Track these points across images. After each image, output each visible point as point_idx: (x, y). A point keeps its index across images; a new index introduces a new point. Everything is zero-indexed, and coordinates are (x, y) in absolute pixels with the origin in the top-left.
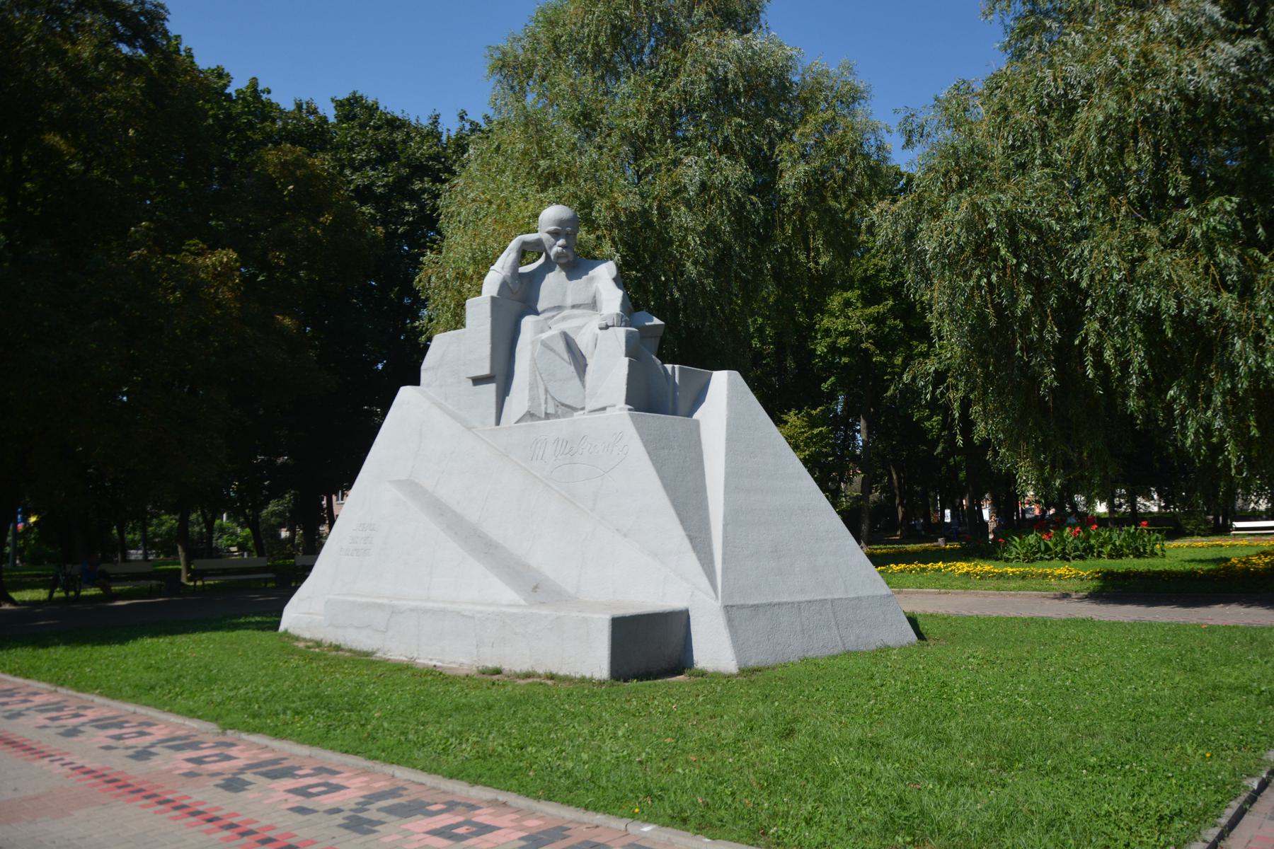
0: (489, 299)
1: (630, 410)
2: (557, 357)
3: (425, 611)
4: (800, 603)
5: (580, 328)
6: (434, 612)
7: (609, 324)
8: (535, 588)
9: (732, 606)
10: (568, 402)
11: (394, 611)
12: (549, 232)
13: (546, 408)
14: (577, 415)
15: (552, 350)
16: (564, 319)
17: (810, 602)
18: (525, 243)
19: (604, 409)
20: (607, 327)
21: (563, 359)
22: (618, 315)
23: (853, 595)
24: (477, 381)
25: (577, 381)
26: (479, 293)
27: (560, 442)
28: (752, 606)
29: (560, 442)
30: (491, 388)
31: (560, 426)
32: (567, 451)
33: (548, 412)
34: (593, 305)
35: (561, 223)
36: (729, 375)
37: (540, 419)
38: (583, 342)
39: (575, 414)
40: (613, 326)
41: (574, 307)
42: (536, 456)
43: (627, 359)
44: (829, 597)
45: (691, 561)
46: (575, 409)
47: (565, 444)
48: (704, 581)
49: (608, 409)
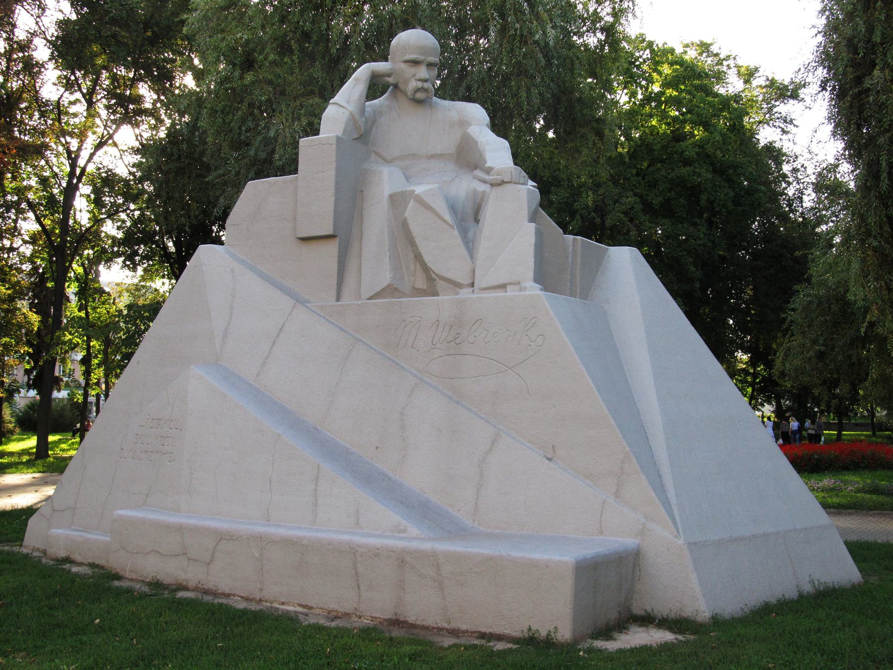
7: (505, 180)
10: (450, 275)
14: (465, 293)
15: (428, 207)
19: (503, 287)
21: (444, 221)
33: (417, 286)
35: (423, 50)
37: (404, 295)
43: (533, 225)
49: (509, 288)
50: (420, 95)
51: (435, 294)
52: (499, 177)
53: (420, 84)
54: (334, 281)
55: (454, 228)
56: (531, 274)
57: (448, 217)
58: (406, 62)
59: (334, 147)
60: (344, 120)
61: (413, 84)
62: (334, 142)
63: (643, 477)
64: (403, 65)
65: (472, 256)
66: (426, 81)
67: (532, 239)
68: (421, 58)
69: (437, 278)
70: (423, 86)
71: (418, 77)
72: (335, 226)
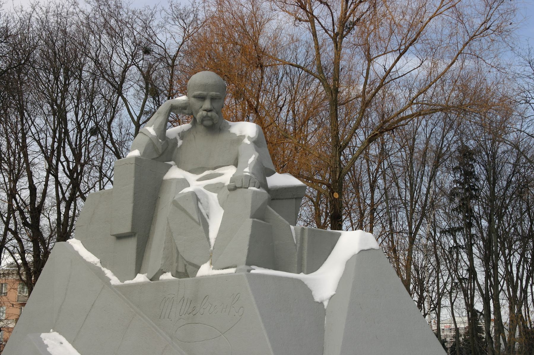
7: (237, 186)
12: (195, 97)
13: (177, 267)
20: (235, 188)
21: (193, 219)
24: (120, 237)
30: (131, 244)
40: (241, 187)
47: (189, 302)
50: (208, 123)
51: (188, 276)
52: (234, 183)
55: (200, 225)
56: (244, 259)
58: (195, 97)
59: (133, 166)
61: (202, 113)
62: (133, 161)
64: (193, 100)
66: (210, 111)
67: (248, 231)
68: (205, 93)
69: (187, 264)
70: (207, 114)
71: (203, 108)
72: (133, 225)
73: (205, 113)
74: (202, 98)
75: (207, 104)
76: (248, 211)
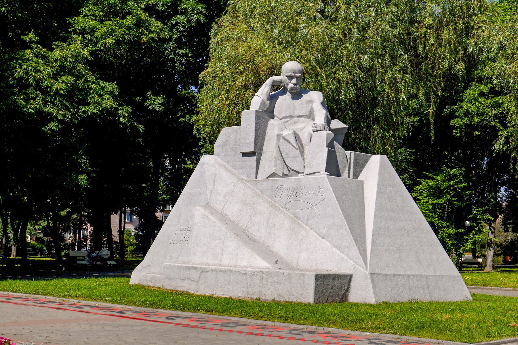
0: (255, 112)
1: (327, 175)
2: (291, 145)
3: (221, 271)
4: (409, 276)
5: (302, 129)
6: (225, 271)
8: (276, 262)
9: (374, 274)
11: (204, 271)
12: (287, 76)
15: (288, 141)
16: (294, 123)
17: (415, 275)
18: (274, 81)
19: (314, 173)
20: (317, 131)
21: (294, 146)
22: (323, 124)
23: (438, 274)
25: (300, 159)
26: (248, 107)
27: (291, 189)
28: (384, 275)
29: (291, 189)
30: (254, 158)
31: (291, 181)
32: (294, 194)
34: (311, 116)
36: (381, 157)
37: (280, 176)
38: (304, 137)
39: (299, 175)
41: (299, 116)
42: (277, 195)
43: (327, 148)
44: (425, 274)
45: (355, 251)
46: (299, 173)
48: (361, 262)
53: (293, 85)
54: (255, 171)
56: (324, 168)
57: (295, 145)
58: (287, 76)
60: (259, 103)
63: (357, 248)
65: (304, 161)
67: (326, 154)
73: (293, 85)
74: (290, 78)
75: (294, 81)
76: (325, 143)
